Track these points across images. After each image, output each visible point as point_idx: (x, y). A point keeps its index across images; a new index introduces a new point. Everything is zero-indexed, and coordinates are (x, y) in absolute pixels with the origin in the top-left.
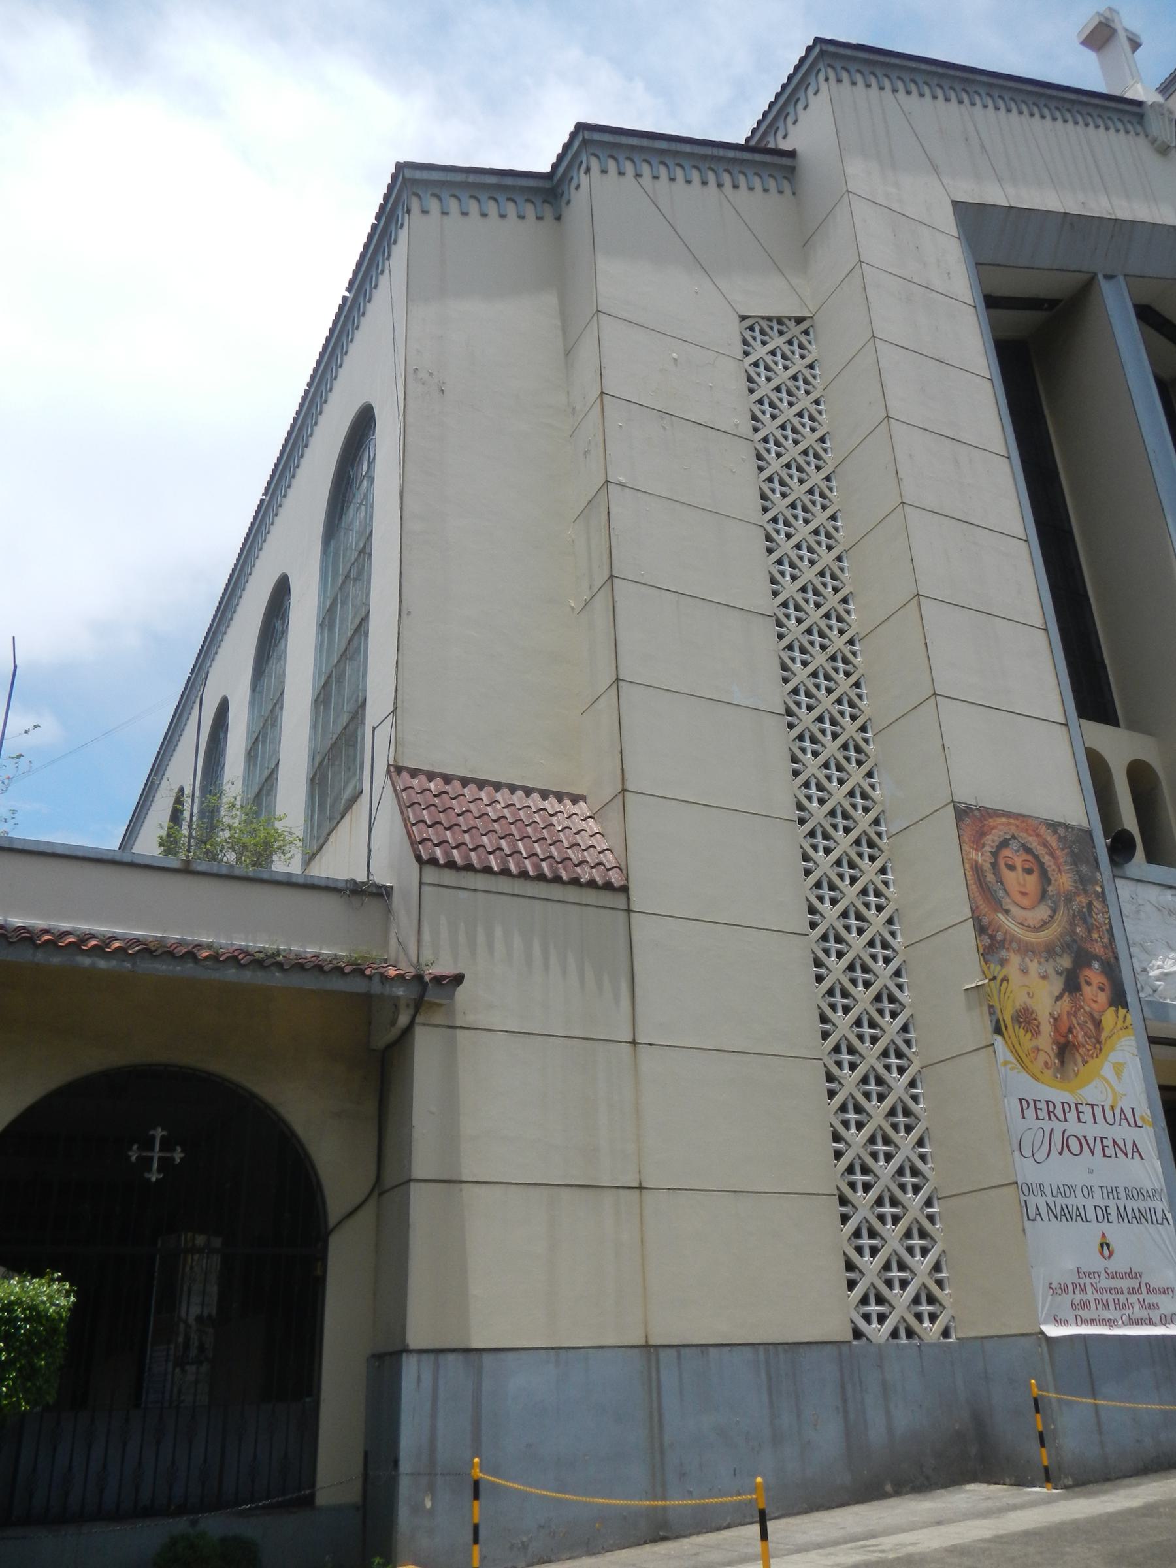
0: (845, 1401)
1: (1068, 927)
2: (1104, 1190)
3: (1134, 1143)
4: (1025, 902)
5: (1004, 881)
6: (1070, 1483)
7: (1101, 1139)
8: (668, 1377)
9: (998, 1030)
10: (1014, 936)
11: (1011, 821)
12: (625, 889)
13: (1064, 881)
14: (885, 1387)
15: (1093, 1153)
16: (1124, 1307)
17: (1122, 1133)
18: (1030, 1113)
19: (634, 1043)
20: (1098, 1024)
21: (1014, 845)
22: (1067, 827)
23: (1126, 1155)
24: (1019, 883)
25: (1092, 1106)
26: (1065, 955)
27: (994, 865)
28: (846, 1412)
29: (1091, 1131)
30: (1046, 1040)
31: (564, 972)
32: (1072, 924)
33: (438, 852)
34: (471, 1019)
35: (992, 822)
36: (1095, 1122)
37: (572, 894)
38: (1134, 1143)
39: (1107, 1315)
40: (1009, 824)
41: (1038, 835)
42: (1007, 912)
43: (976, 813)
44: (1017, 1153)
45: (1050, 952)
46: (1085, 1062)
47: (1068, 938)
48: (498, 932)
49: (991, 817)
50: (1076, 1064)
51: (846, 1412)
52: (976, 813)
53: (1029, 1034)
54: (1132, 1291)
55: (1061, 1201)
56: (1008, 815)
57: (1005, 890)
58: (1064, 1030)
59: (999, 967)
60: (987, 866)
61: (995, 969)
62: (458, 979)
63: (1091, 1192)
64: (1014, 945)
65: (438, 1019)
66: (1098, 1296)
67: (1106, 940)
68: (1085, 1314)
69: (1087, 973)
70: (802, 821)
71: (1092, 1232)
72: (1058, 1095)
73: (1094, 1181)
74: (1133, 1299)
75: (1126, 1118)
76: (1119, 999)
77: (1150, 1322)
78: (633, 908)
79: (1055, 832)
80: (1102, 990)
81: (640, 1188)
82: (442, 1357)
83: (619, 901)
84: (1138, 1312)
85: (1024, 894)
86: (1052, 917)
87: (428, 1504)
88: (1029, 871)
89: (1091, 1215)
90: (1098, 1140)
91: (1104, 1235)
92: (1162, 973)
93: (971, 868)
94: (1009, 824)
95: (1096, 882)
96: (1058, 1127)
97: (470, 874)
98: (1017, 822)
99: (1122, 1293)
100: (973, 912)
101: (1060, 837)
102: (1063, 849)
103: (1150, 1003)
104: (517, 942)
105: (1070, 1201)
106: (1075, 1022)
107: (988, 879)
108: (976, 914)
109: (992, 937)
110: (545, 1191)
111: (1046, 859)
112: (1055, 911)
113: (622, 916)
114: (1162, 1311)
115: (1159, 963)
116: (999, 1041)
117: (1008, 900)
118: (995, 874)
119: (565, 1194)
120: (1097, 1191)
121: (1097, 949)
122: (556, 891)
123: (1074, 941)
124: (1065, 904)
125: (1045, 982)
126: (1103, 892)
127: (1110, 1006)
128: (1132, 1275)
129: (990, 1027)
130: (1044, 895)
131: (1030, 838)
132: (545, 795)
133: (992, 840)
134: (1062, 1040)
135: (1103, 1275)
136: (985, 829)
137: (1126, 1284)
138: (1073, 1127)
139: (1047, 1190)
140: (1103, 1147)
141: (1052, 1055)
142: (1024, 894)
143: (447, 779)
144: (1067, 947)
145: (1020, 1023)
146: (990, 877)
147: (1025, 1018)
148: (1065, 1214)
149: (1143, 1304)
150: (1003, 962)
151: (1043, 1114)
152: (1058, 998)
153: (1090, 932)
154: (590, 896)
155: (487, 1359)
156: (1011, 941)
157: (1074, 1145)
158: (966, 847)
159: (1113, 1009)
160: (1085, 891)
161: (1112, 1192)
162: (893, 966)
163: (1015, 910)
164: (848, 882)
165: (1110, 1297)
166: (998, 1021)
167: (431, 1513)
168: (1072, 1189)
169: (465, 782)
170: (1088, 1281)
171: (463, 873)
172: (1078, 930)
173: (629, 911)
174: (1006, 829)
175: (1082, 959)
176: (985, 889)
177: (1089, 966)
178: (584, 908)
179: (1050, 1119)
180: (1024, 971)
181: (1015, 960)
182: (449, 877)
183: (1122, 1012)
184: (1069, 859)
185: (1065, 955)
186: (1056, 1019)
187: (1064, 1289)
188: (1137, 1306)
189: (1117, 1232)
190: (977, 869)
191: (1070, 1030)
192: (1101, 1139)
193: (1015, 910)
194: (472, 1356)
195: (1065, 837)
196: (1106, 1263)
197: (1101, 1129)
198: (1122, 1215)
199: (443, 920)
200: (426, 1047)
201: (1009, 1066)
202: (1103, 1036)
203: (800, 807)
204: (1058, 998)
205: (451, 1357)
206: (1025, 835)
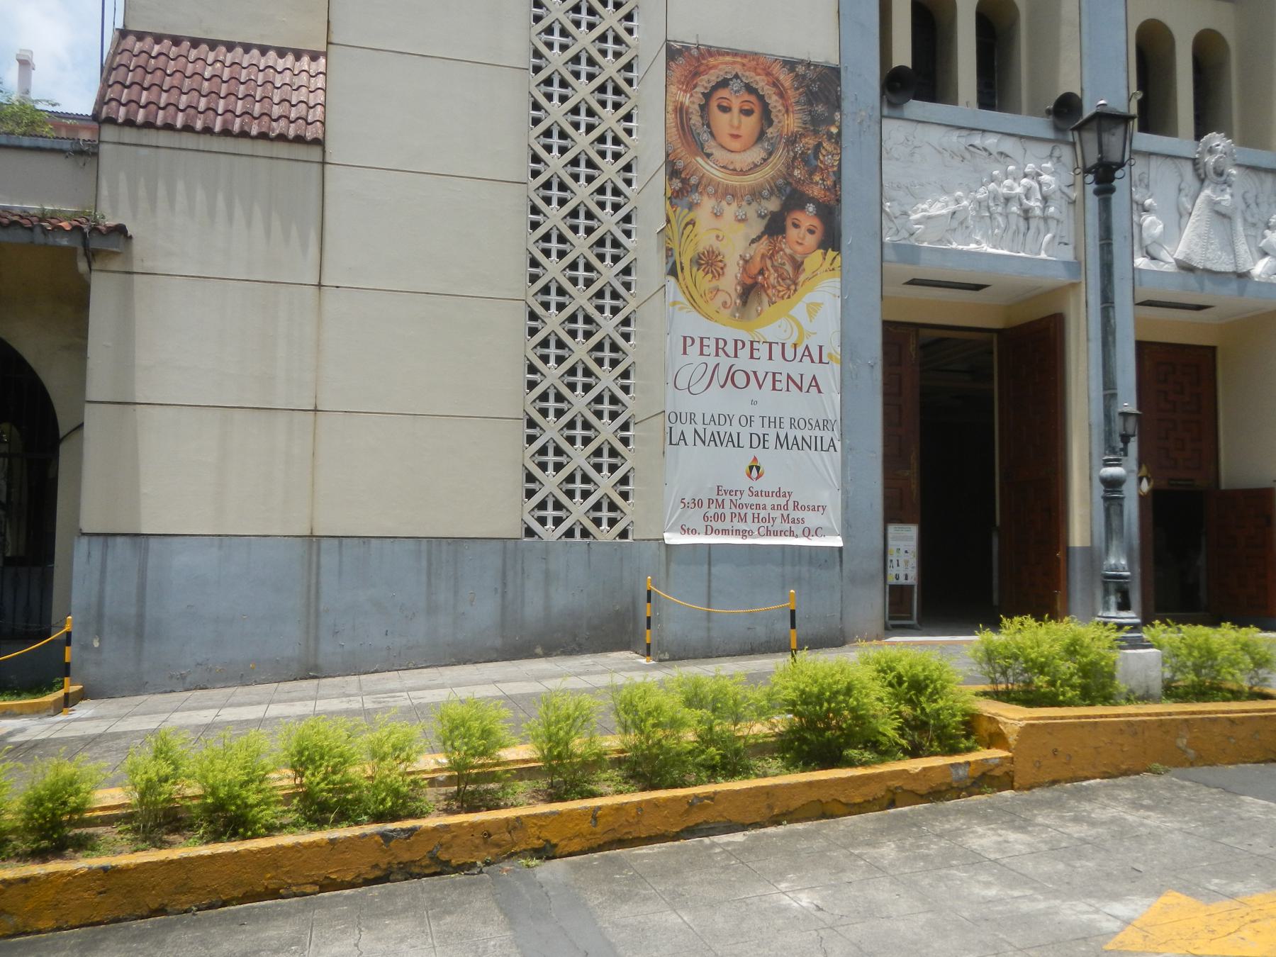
0: (505, 584)
1: (784, 171)
2: (766, 420)
4: (735, 145)
5: (712, 124)
6: (667, 657)
7: (774, 374)
8: (329, 560)
9: (673, 272)
10: (711, 180)
11: (739, 59)
12: (319, 142)
13: (790, 122)
14: (548, 577)
15: (760, 387)
17: (808, 369)
18: (694, 350)
19: (320, 285)
20: (798, 266)
21: (735, 85)
22: (809, 64)
23: (801, 389)
24: (732, 126)
25: (771, 344)
26: (773, 198)
27: (704, 108)
28: (504, 594)
31: (249, 224)
32: (790, 166)
33: (122, 110)
34: (148, 265)
35: (712, 61)
36: (770, 358)
37: (262, 147)
38: (814, 377)
39: (742, 526)
40: (734, 63)
41: (768, 74)
42: (708, 155)
43: (695, 52)
44: (671, 384)
45: (756, 194)
46: (772, 303)
47: (781, 181)
48: (180, 186)
49: (711, 54)
50: (760, 303)
51: (504, 594)
52: (695, 52)
53: (710, 276)
56: (735, 53)
57: (711, 134)
59: (686, 211)
60: (695, 108)
61: (683, 214)
62: (120, 230)
63: (750, 421)
64: (711, 189)
65: (115, 265)
66: (734, 510)
67: (829, 183)
68: (718, 525)
69: (798, 215)
70: (537, 69)
71: (744, 457)
72: (730, 333)
73: (756, 412)
75: (810, 355)
76: (831, 240)
77: (792, 533)
78: (328, 159)
79: (792, 69)
80: (811, 232)
81: (316, 410)
82: (110, 540)
83: (315, 153)
84: (779, 525)
85: (736, 137)
86: (765, 160)
87: (96, 644)
88: (748, 113)
90: (770, 376)
91: (755, 459)
92: (924, 217)
93: (675, 110)
94: (734, 63)
95: (833, 122)
96: (725, 363)
97: (153, 132)
98: (745, 61)
99: (765, 508)
100: (667, 155)
101: (797, 75)
102: (797, 89)
103: (896, 246)
104: (200, 195)
106: (769, 263)
107: (692, 122)
108: (671, 158)
110: (218, 412)
111: (774, 101)
112: (770, 154)
113: (317, 167)
114: (806, 525)
115: (925, 206)
116: (672, 279)
117: (713, 143)
118: (702, 117)
119: (238, 415)
121: (816, 191)
122: (244, 146)
123: (789, 184)
124: (786, 145)
125: (742, 225)
126: (839, 134)
127: (819, 248)
130: (761, 136)
131: (758, 78)
132: (282, 53)
133: (705, 82)
134: (749, 281)
135: (747, 492)
136: (702, 68)
137: (769, 501)
138: (743, 361)
139: (699, 419)
140: (774, 381)
141: (734, 295)
142: (736, 137)
143: (176, 41)
144: (775, 190)
145: (700, 265)
146: (696, 119)
147: (709, 262)
148: (716, 439)
149: (785, 519)
150: (691, 206)
152: (753, 241)
153: (811, 174)
154: (281, 150)
156: (706, 186)
157: (740, 379)
158: (673, 89)
159: (821, 251)
160: (816, 132)
161: (776, 422)
162: (622, 213)
163: (718, 154)
164: (583, 129)
165: (750, 512)
166: (674, 263)
167: (99, 650)
169: (195, 43)
170: (727, 498)
171: (145, 131)
172: (796, 172)
173: (323, 163)
174: (728, 68)
175: (794, 199)
176: (689, 131)
177: (802, 208)
178: (275, 161)
179: (717, 355)
180: (717, 215)
181: (708, 204)
182: (129, 135)
183: (831, 254)
184: (803, 99)
185: (773, 198)
186: (746, 262)
187: (698, 503)
188: (778, 520)
190: (681, 111)
193: (718, 154)
194: (138, 539)
195: (804, 77)
196: (749, 483)
197: (778, 364)
198: (781, 442)
199: (122, 176)
200: (103, 289)
201: (677, 307)
202: (802, 278)
203: (537, 54)
204: (753, 241)
205: (119, 540)
206: (752, 74)
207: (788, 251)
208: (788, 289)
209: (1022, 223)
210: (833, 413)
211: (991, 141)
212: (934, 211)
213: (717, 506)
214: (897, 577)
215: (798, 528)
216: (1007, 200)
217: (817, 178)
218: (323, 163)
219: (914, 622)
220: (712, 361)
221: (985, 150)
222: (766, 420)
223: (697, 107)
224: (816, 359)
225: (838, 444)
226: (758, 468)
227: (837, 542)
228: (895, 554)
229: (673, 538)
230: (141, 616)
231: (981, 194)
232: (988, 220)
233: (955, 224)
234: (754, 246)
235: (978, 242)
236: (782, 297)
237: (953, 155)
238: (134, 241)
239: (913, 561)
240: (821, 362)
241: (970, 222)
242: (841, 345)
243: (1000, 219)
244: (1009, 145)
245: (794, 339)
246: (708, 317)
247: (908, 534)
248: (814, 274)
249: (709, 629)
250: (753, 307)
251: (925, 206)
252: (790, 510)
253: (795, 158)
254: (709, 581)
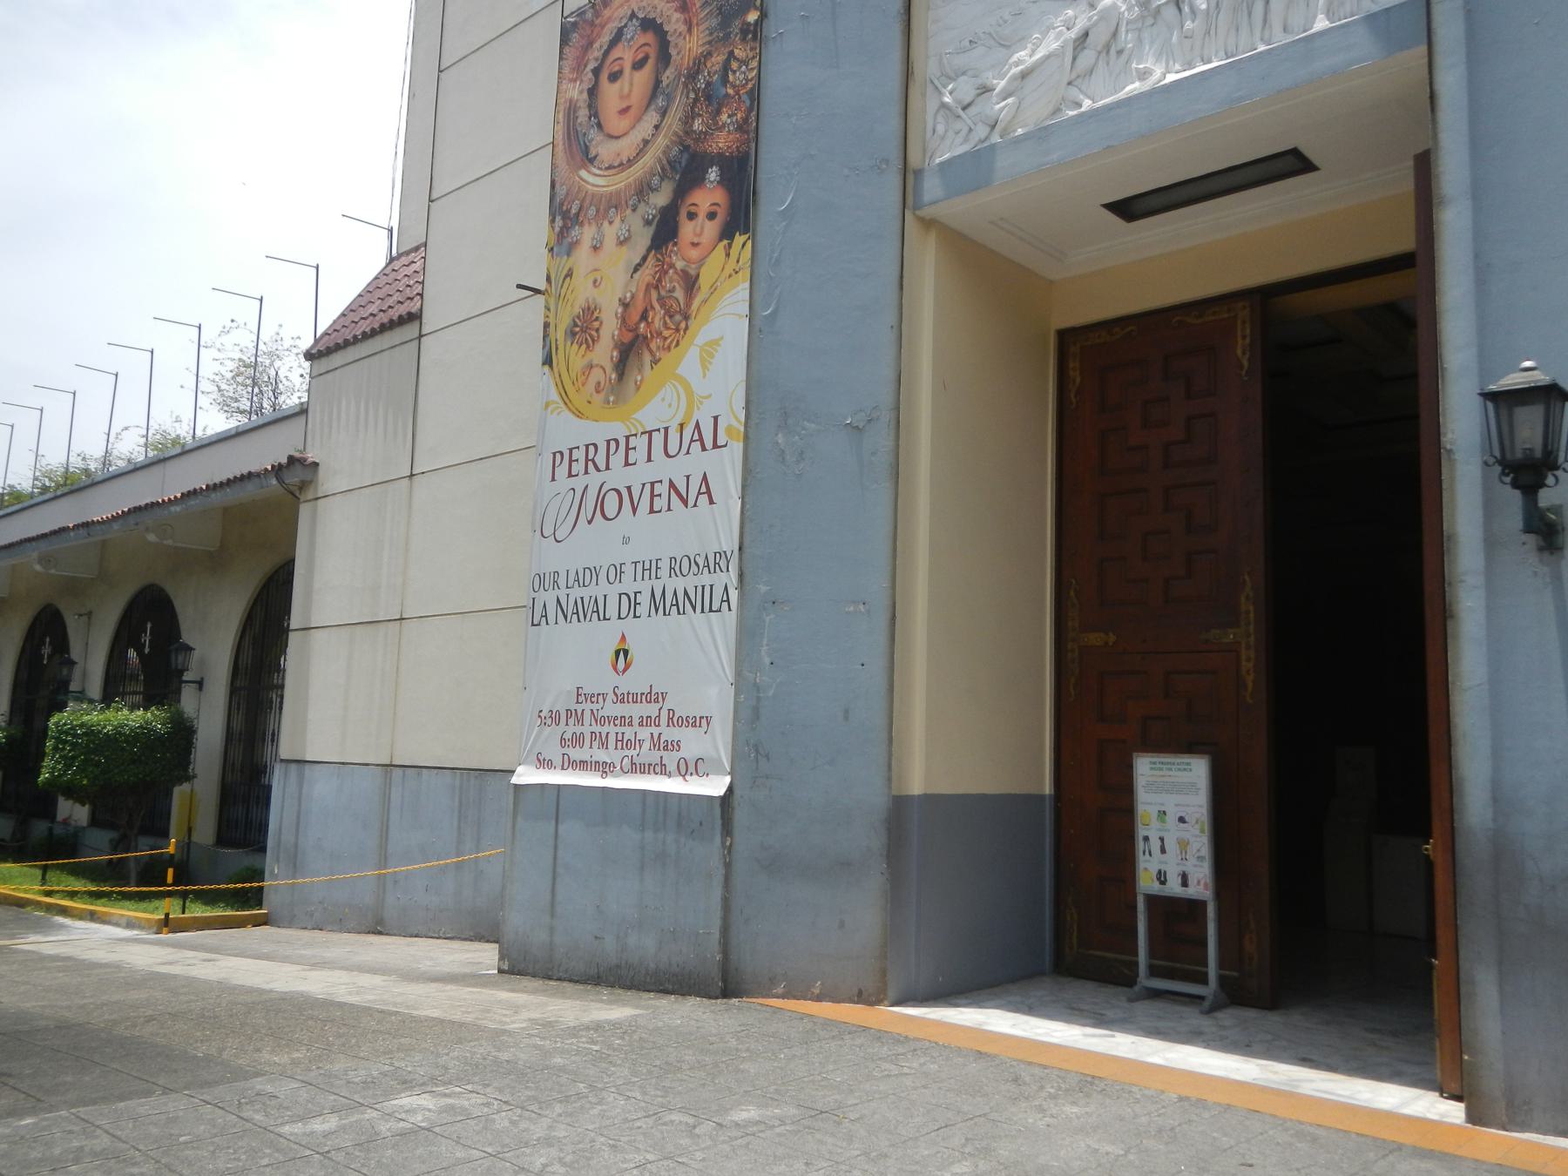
3: (705, 478)
7: (652, 484)
16: (629, 744)
20: (691, 283)
27: (593, 92)
29: (639, 475)
30: (604, 352)
38: (705, 478)
39: (601, 756)
45: (643, 190)
46: (656, 361)
50: (640, 371)
54: (645, 721)
55: (577, 592)
58: (635, 316)
61: (565, 263)
63: (619, 571)
66: (597, 729)
68: (576, 754)
71: (605, 636)
72: (599, 431)
73: (627, 555)
74: (644, 733)
75: (701, 439)
76: (739, 218)
77: (661, 769)
80: (711, 216)
84: (647, 754)
86: (657, 127)
89: (612, 611)
90: (648, 487)
91: (623, 638)
92: (1014, 78)
96: (594, 479)
105: (585, 593)
109: (565, 215)
110: (344, 631)
112: (664, 113)
114: (683, 753)
118: (590, 106)
120: (629, 569)
128: (652, 697)
129: (539, 356)
135: (611, 696)
137: (636, 710)
138: (618, 476)
146: (583, 113)
149: (656, 743)
151: (578, 467)
155: (307, 766)
159: (725, 242)
161: (649, 569)
168: (594, 572)
170: (588, 706)
179: (586, 472)
187: (555, 717)
189: (644, 633)
190: (571, 110)
191: (644, 317)
192: (652, 484)
207: (680, 265)
208: (677, 330)
210: (728, 541)
213: (575, 723)
214: (1162, 878)
215: (670, 759)
217: (724, 117)
218: (421, 336)
219: (1210, 990)
220: (578, 483)
222: (639, 567)
223: (585, 95)
224: (709, 443)
225: (734, 595)
226: (626, 652)
227: (715, 786)
228: (1155, 824)
229: (527, 775)
230: (296, 845)
233: (1087, 57)
234: (636, 276)
235: (1143, 75)
236: (669, 348)
238: (321, 469)
239: (1201, 844)
240: (715, 446)
241: (1127, 39)
242: (747, 408)
245: (678, 420)
246: (579, 414)
247: (1182, 777)
248: (713, 289)
249: (552, 929)
250: (633, 376)
252: (654, 724)
253: (696, 100)
254: (556, 847)
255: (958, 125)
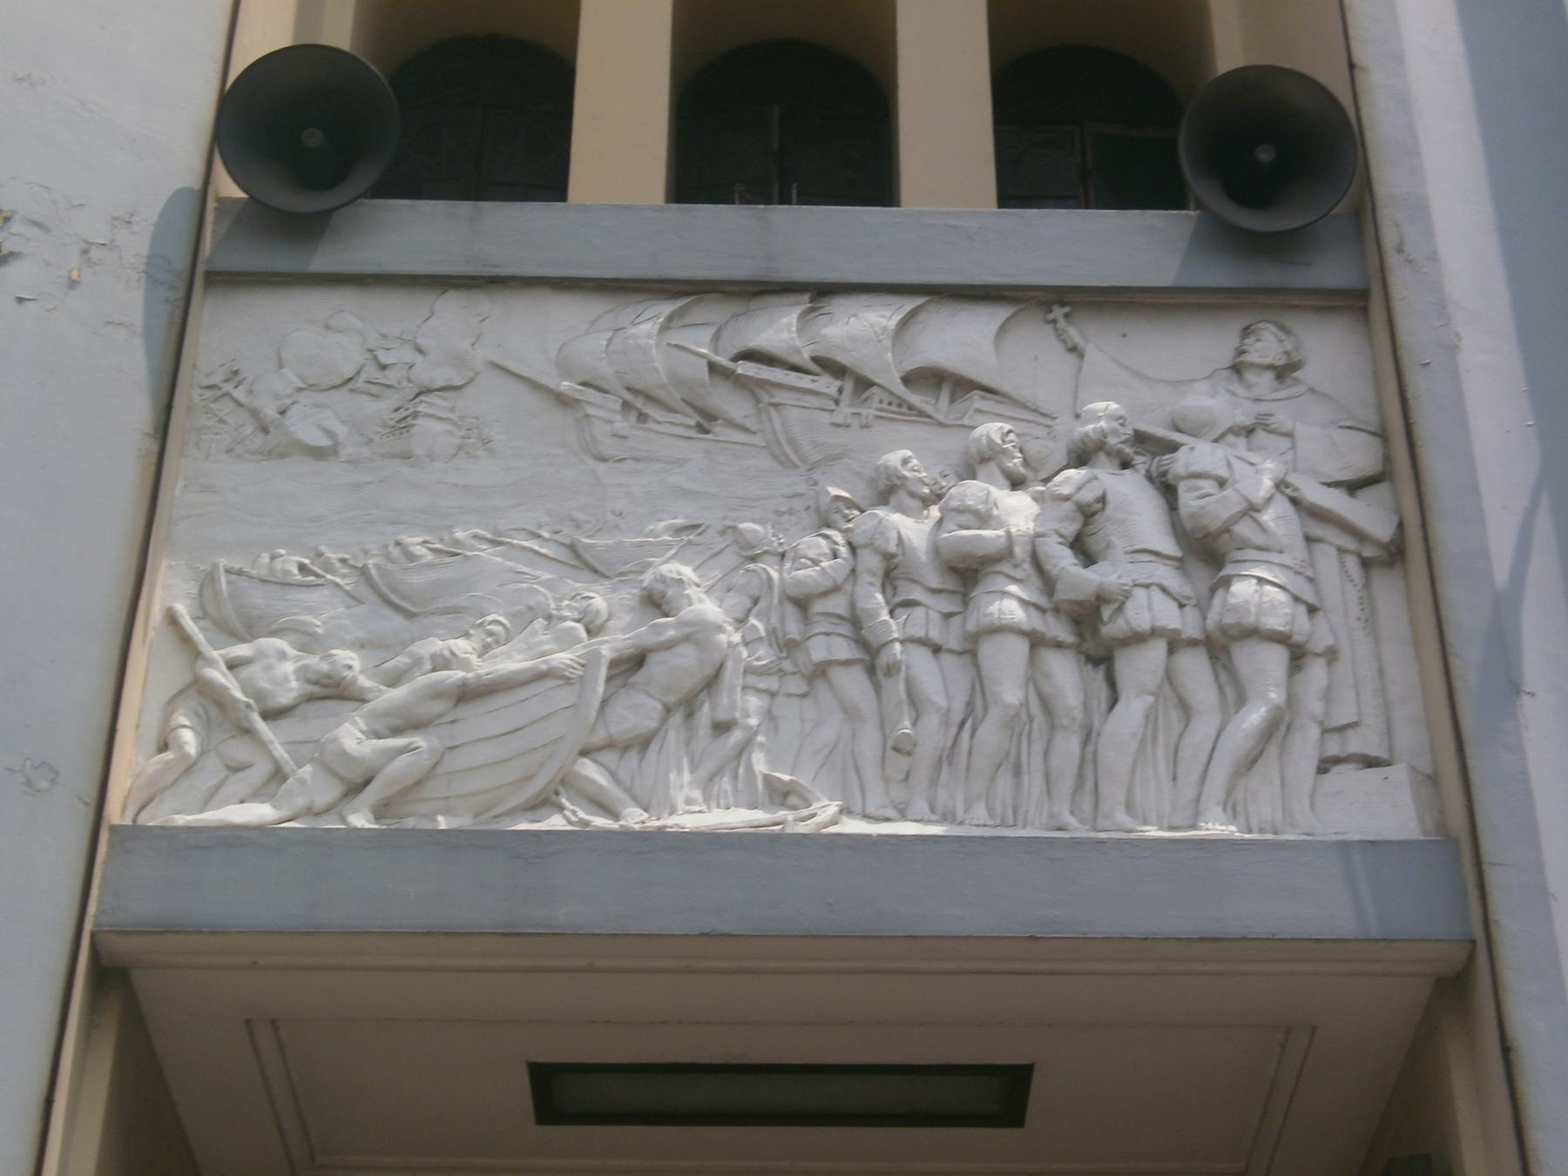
92: (437, 693)
209: (1066, 676)
211: (860, 328)
212: (509, 662)
216: (967, 573)
221: (829, 366)
231: (817, 557)
232: (853, 683)
233: (637, 711)
237: (640, 400)
243: (923, 666)
244: (962, 339)
251: (461, 645)
255: (240, 750)
